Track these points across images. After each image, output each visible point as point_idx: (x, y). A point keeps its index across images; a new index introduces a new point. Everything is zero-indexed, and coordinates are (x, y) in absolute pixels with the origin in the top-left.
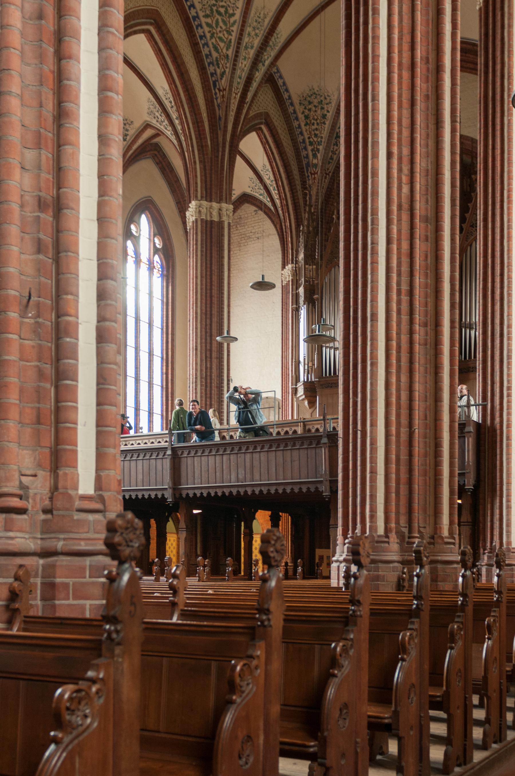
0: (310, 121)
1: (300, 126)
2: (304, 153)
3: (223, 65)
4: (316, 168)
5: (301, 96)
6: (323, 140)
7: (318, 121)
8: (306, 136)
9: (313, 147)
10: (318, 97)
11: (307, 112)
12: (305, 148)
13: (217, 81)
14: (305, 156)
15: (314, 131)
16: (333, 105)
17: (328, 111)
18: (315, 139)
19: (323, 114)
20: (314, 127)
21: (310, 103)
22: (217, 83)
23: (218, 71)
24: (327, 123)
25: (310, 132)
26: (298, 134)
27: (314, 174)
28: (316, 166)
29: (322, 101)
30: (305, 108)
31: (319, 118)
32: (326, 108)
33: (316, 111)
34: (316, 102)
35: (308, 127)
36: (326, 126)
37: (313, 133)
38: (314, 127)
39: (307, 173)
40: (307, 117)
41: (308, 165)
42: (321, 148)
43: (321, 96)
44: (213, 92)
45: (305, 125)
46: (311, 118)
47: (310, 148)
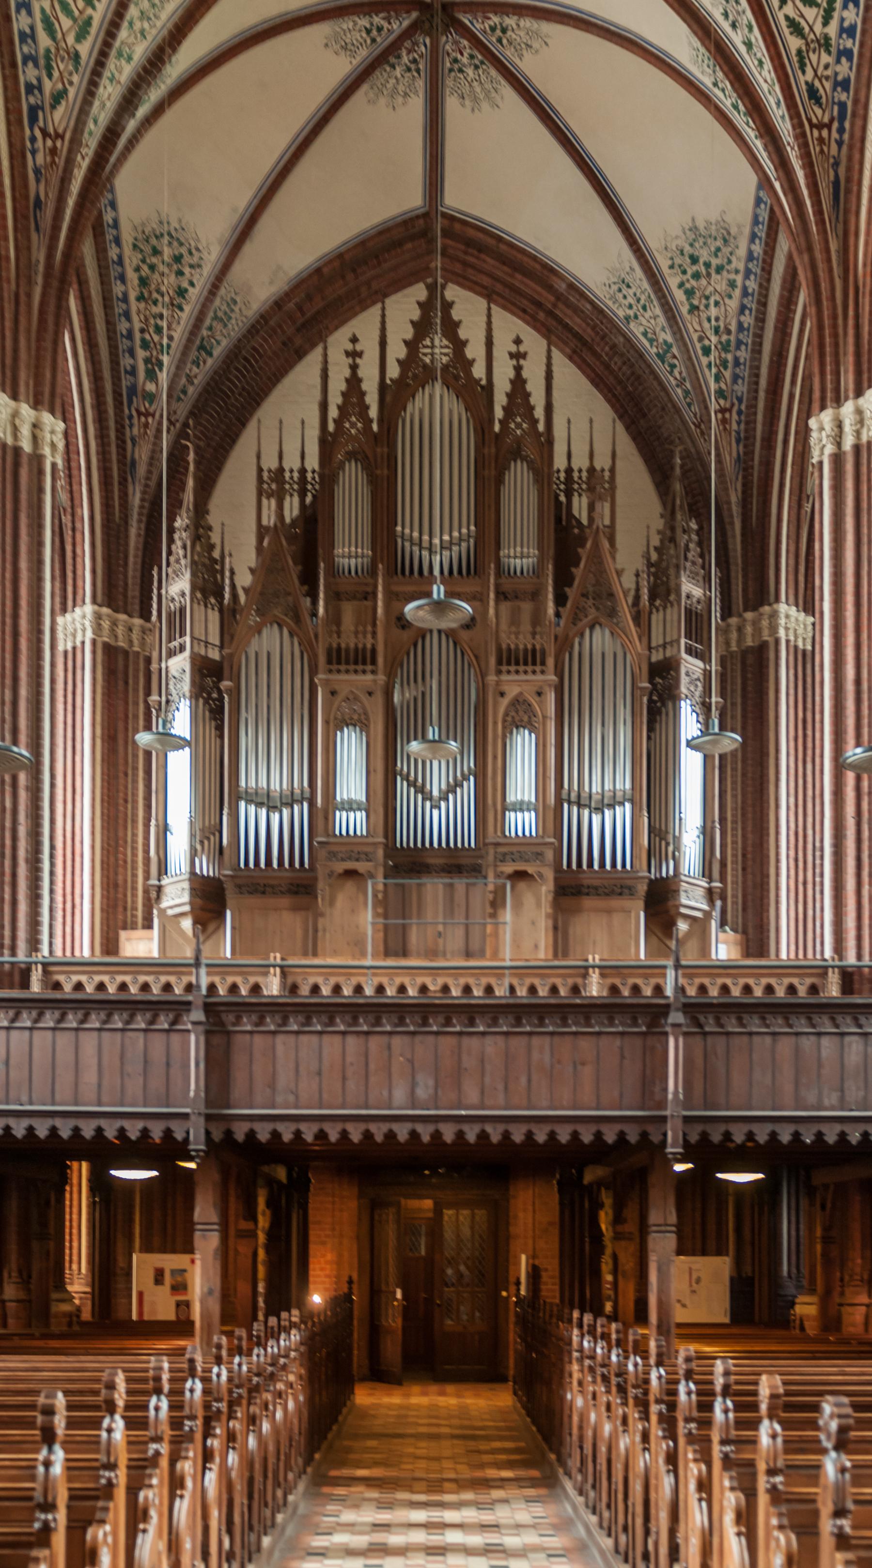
0: (150, 293)
3: (60, 73)
4: (151, 403)
5: (140, 229)
6: (174, 345)
9: (148, 354)
13: (43, 109)
15: (155, 317)
18: (156, 338)
20: (155, 310)
22: (40, 114)
23: (48, 85)
25: (146, 319)
27: (147, 414)
30: (144, 261)
37: (152, 321)
38: (155, 310)
40: (144, 282)
42: (165, 359)
44: (28, 132)
45: (140, 298)
46: (153, 286)
47: (141, 354)
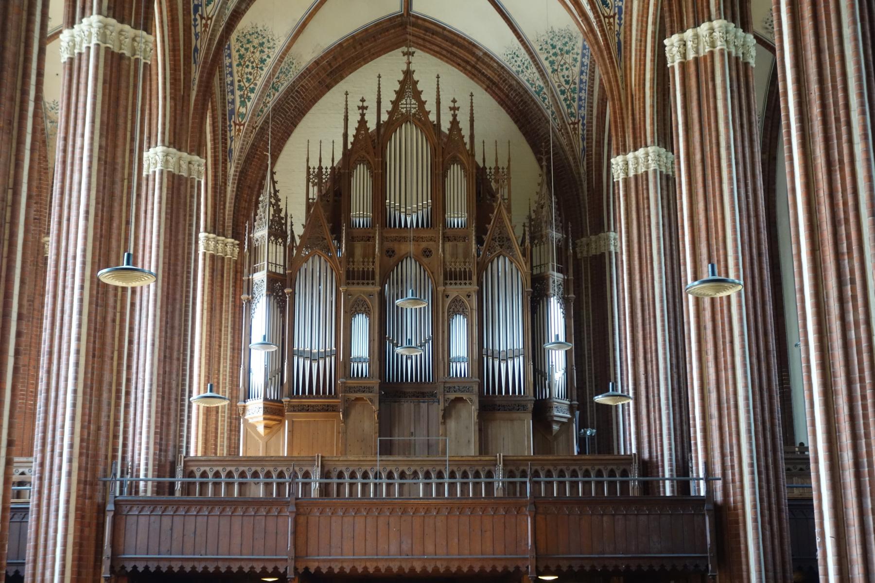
1: (231, 66)
2: (230, 97)
4: (243, 119)
7: (254, 65)
8: (236, 79)
9: (242, 93)
10: (260, 37)
11: (243, 51)
12: (233, 92)
14: (230, 100)
15: (247, 74)
16: (276, 51)
17: (269, 57)
18: (247, 85)
19: (261, 58)
21: (249, 42)
25: (242, 75)
26: (227, 74)
27: (240, 125)
28: (243, 116)
29: (263, 43)
30: (242, 46)
31: (257, 61)
32: (266, 53)
33: (253, 52)
34: (256, 42)
35: (240, 68)
36: (264, 73)
39: (230, 122)
40: (241, 57)
41: (232, 112)
42: (252, 96)
43: (264, 38)
45: (238, 65)
47: (238, 93)
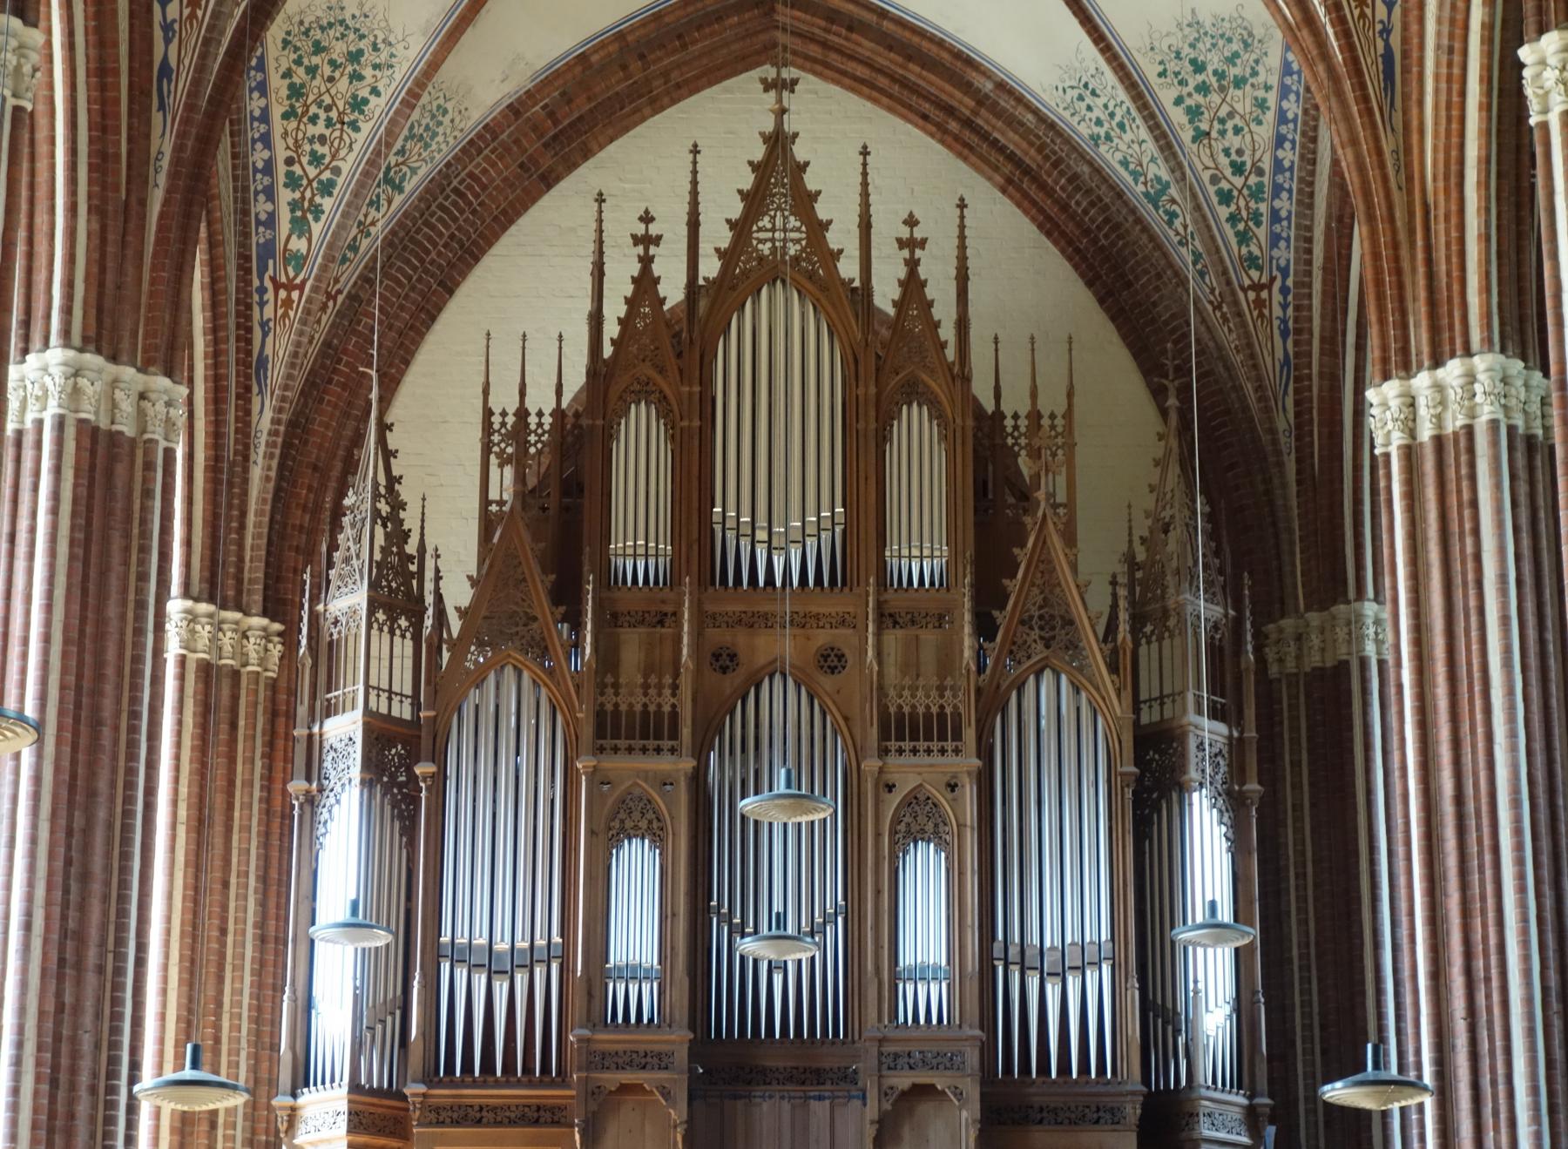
1: (265, 117)
2: (261, 207)
5: (296, 19)
7: (334, 114)
8: (281, 154)
9: (297, 195)
10: (352, 36)
11: (300, 75)
12: (270, 193)
14: (263, 217)
15: (311, 141)
16: (398, 76)
17: (375, 91)
18: (312, 172)
19: (355, 97)
21: (318, 48)
24: (366, 128)
25: (297, 145)
27: (290, 287)
28: (300, 261)
29: (360, 52)
30: (298, 62)
31: (341, 104)
32: (369, 80)
33: (331, 79)
34: (339, 50)
35: (293, 124)
36: (361, 137)
39: (261, 279)
40: (296, 92)
41: (268, 250)
42: (327, 203)
43: (362, 37)
45: (286, 116)
47: (285, 196)
